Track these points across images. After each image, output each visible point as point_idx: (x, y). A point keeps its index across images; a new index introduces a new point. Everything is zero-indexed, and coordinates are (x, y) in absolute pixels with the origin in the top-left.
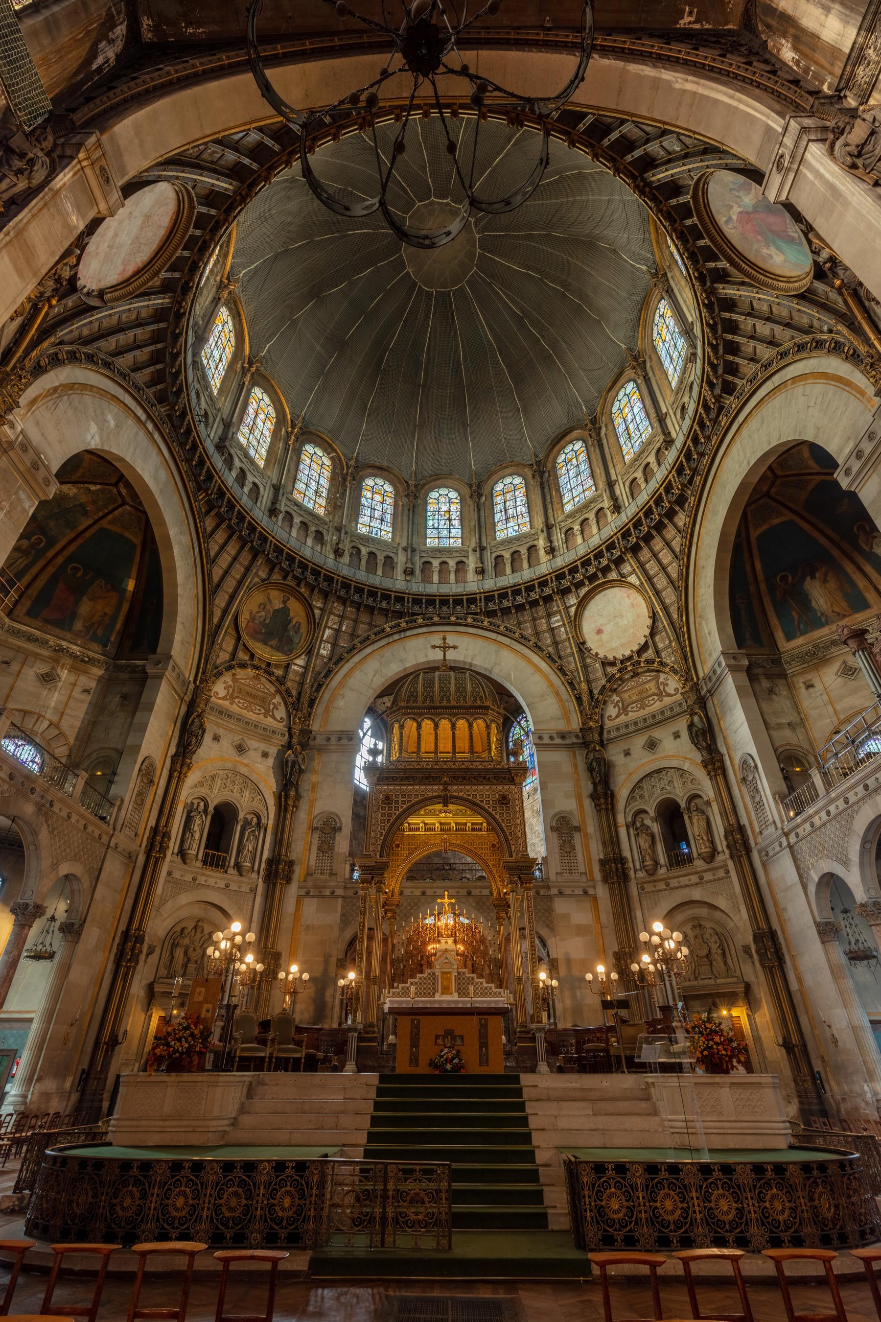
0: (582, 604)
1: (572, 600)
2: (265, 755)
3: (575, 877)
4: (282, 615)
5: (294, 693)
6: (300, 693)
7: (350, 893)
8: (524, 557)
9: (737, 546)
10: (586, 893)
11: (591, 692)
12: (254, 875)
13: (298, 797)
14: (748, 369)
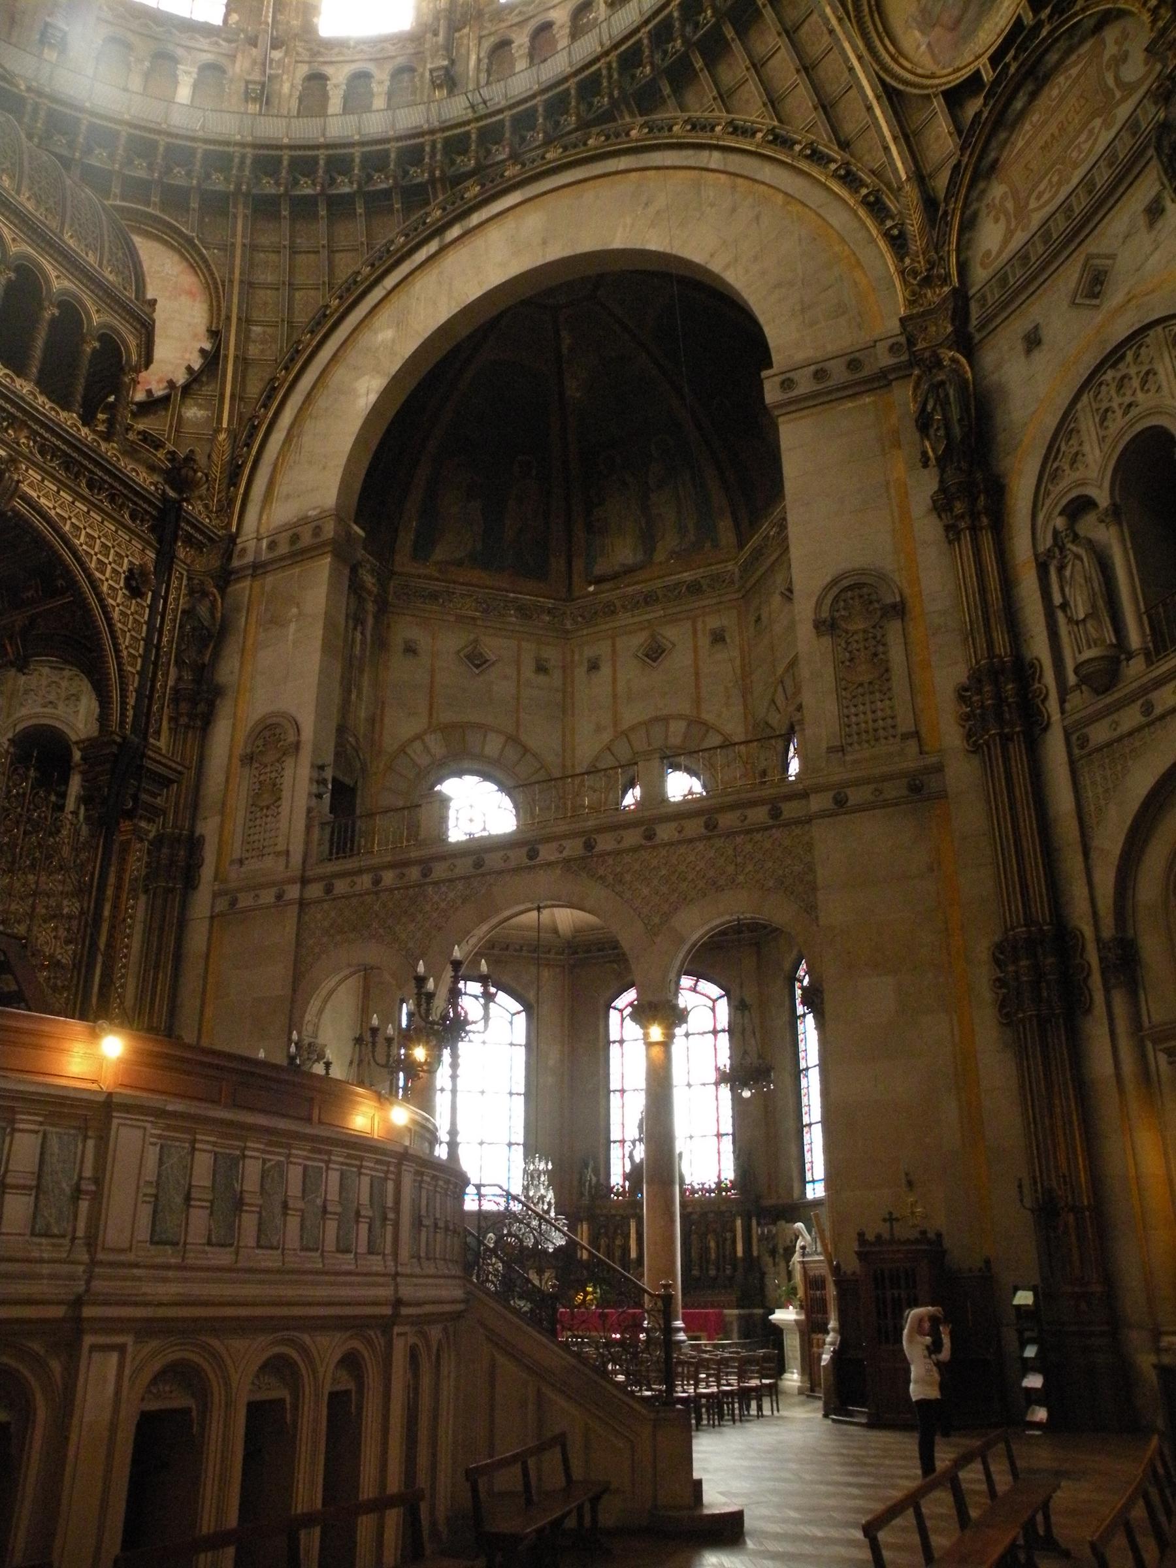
9: (456, 350)
14: (701, 102)
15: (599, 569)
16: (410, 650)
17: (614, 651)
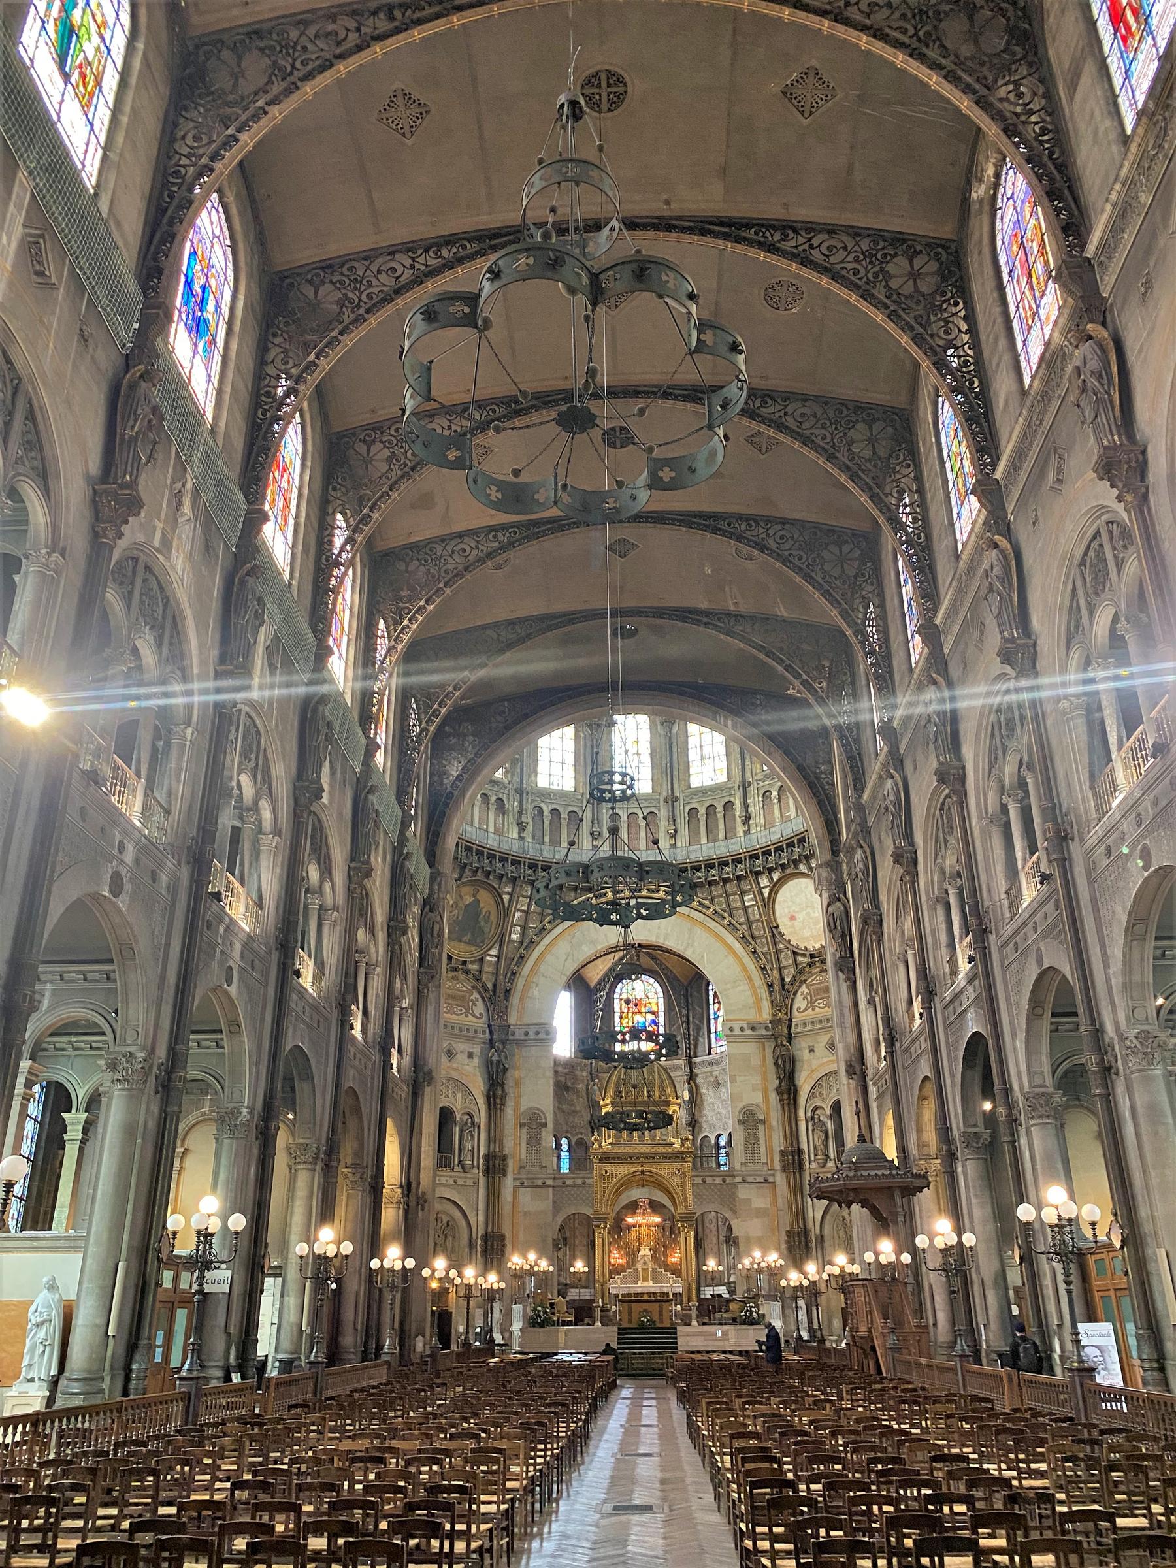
0: (775, 887)
1: (764, 881)
2: (470, 1055)
3: (758, 1166)
4: (473, 911)
5: (490, 986)
6: (495, 986)
7: (559, 1183)
8: (720, 815)
10: (766, 1180)
11: (783, 980)
12: (475, 1170)
13: (504, 1096)
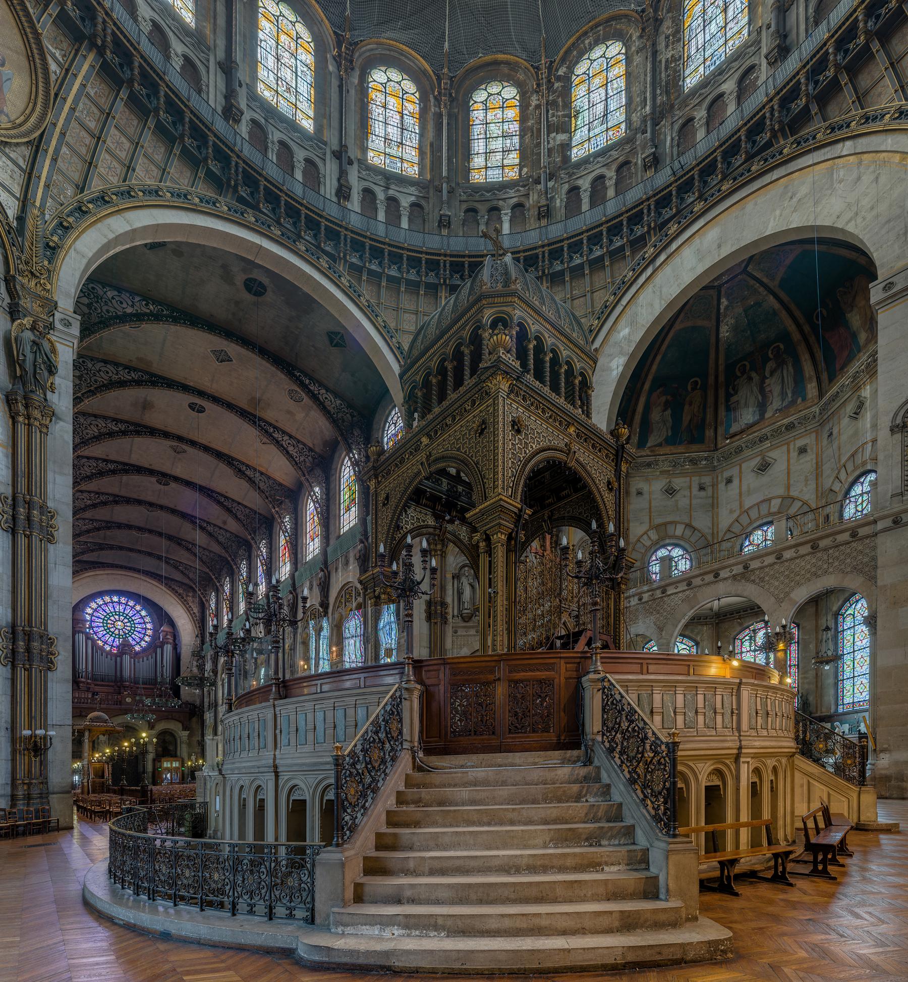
15: (734, 428)
16: (639, 493)
17: (740, 472)
